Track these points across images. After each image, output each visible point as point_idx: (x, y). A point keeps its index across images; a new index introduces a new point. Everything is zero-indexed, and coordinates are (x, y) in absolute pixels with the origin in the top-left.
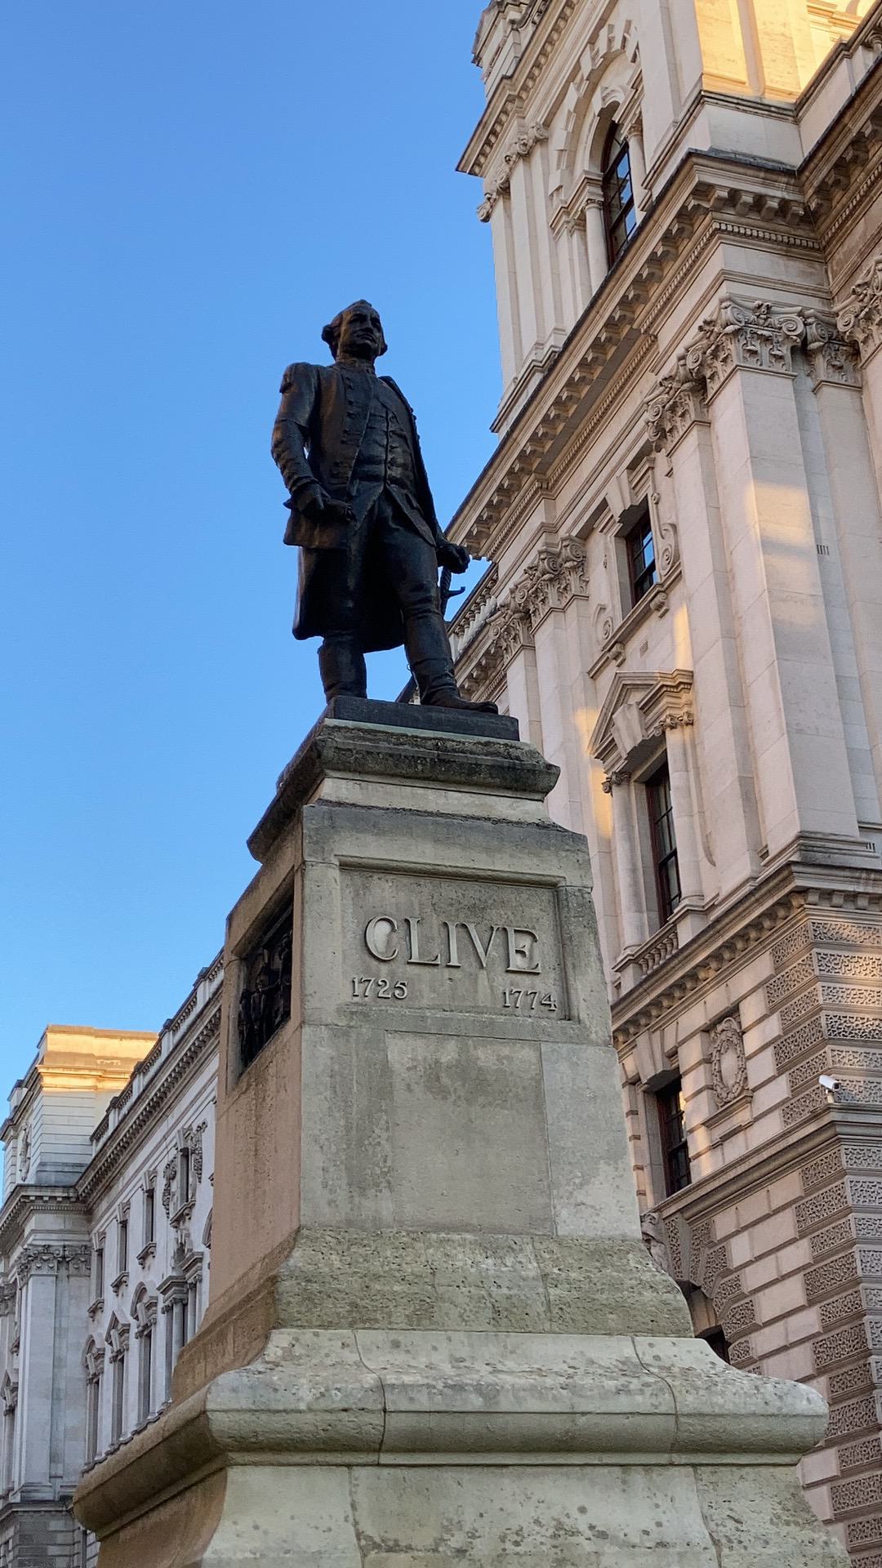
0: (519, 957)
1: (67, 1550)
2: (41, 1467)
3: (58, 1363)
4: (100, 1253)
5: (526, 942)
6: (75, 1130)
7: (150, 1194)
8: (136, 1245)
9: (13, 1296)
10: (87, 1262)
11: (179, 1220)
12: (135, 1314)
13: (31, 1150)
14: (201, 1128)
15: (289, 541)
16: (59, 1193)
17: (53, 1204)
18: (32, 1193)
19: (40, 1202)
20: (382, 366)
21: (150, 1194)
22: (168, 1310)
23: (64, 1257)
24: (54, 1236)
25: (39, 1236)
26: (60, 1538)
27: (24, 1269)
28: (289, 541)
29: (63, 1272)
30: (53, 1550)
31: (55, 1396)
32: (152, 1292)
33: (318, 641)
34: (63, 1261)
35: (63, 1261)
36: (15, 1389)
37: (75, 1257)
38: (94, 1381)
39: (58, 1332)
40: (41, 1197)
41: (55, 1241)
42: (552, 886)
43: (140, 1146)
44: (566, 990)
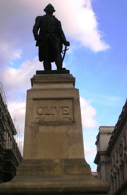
0: (65, 112)
4: (111, 161)
5: (66, 109)
7: (117, 152)
8: (116, 160)
11: (121, 156)
12: (117, 171)
14: (122, 141)
15: (36, 46)
16: (104, 153)
20: (54, 14)
21: (117, 152)
22: (121, 170)
24: (104, 159)
28: (36, 46)
32: (118, 167)
33: (43, 61)
35: (106, 163)
38: (113, 181)
41: (104, 160)
42: (72, 99)
43: (115, 144)
44: (74, 116)
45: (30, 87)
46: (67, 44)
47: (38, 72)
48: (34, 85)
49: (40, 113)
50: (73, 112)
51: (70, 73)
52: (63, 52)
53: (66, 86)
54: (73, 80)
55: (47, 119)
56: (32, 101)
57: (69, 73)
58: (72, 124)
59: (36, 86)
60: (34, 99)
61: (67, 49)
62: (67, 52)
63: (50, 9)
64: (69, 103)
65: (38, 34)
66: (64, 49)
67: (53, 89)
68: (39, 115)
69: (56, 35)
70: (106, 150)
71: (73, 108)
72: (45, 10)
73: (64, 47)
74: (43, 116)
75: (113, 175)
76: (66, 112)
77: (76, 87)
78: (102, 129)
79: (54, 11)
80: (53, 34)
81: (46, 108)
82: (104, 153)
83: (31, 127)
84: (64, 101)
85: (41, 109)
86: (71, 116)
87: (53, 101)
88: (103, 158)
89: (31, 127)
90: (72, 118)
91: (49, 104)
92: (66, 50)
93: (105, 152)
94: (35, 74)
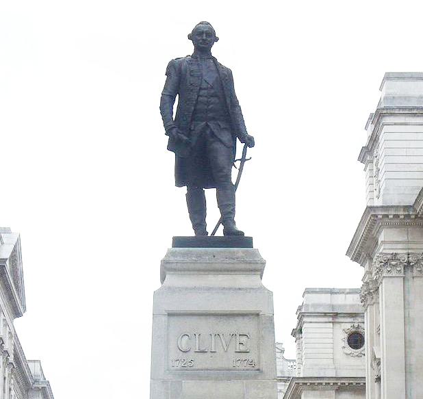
5: (243, 339)
9: (377, 289)
13: (380, 175)
16: (401, 213)
17: (397, 221)
19: (387, 220)
23: (409, 262)
24: (400, 246)
25: (387, 246)
27: (379, 270)
29: (409, 274)
36: (379, 364)
40: (387, 216)
41: (401, 251)
44: (259, 357)
46: (249, 142)
47: (179, 242)
49: (184, 348)
53: (243, 281)
54: (259, 266)
55: (201, 362)
56: (164, 319)
58: (255, 377)
59: (172, 280)
60: (170, 315)
61: (246, 158)
62: (246, 162)
63: (203, 38)
65: (174, 117)
66: (239, 155)
67: (213, 290)
68: (181, 353)
69: (222, 127)
70: (410, 200)
72: (190, 37)
73: (240, 146)
74: (191, 355)
76: (242, 348)
78: (398, 88)
79: (217, 39)
80: (211, 125)
81: (197, 336)
82: (401, 213)
83: (164, 382)
84: (240, 320)
87: (212, 320)
88: (391, 241)
89: (164, 382)
91: (205, 326)
92: (243, 160)
93: (406, 208)
94: (170, 246)
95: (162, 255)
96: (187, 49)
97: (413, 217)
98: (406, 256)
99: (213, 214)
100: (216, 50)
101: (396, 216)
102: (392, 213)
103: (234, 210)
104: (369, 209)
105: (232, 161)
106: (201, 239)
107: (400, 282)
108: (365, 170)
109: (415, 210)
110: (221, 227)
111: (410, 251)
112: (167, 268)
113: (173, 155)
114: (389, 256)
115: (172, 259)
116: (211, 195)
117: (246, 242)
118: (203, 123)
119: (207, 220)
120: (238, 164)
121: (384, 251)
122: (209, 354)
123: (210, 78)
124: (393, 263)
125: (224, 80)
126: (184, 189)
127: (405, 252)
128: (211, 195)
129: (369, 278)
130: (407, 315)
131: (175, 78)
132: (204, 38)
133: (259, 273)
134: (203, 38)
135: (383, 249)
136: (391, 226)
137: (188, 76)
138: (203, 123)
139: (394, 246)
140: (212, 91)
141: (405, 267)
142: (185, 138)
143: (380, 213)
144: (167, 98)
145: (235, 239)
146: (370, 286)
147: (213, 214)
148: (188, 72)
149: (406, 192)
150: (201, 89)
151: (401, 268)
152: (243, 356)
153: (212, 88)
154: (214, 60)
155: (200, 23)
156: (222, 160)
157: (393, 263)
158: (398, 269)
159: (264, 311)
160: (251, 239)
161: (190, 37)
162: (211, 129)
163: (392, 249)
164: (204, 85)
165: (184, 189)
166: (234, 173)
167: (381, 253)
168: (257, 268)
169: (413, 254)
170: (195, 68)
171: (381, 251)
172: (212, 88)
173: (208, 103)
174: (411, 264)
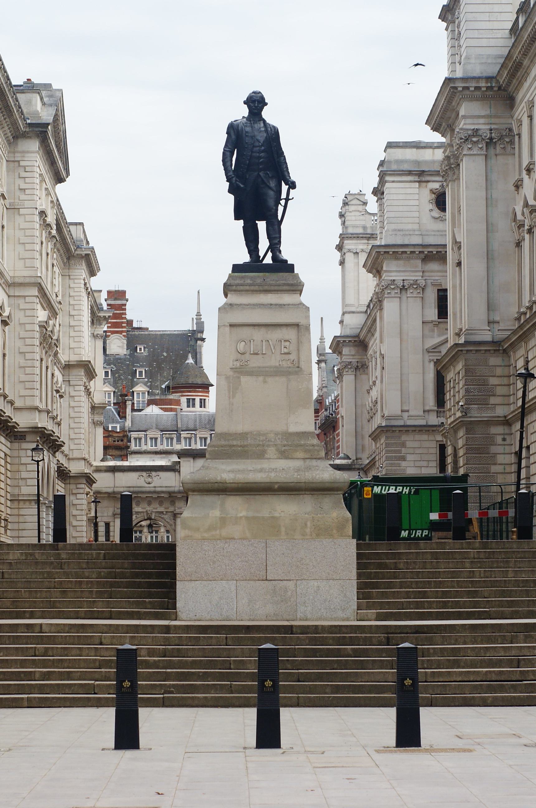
1: (505, 381)
2: (481, 314)
3: (490, 228)
4: (519, 135)
5: (287, 344)
6: (496, 25)
9: (459, 165)
10: (512, 142)
16: (483, 84)
17: (478, 93)
18: (460, 85)
19: (467, 92)
23: (491, 139)
24: (482, 121)
25: (469, 121)
26: (499, 371)
29: (492, 151)
30: (493, 381)
31: (490, 256)
34: (490, 142)
35: (490, 142)
36: (459, 248)
37: (501, 138)
38: (518, 244)
39: (489, 202)
40: (467, 88)
41: (483, 126)
42: (297, 325)
45: (223, 300)
46: (292, 185)
47: (236, 268)
48: (229, 296)
50: (298, 350)
51: (296, 271)
52: (283, 202)
53: (287, 299)
54: (300, 288)
55: (255, 362)
56: (228, 329)
57: (293, 271)
58: (296, 373)
59: (234, 298)
60: (231, 326)
61: (290, 198)
62: (289, 202)
63: (256, 103)
64: (291, 334)
66: (284, 196)
69: (270, 175)
70: (493, 70)
71: (299, 342)
72: (245, 103)
73: (285, 188)
74: (247, 356)
75: (519, 217)
77: (305, 298)
79: (266, 104)
81: (252, 341)
82: (483, 84)
85: (243, 343)
86: (293, 357)
87: (263, 330)
88: (472, 115)
89: (227, 378)
90: (296, 360)
91: (258, 335)
92: (287, 199)
93: (489, 79)
95: (225, 279)
96: (242, 112)
97: (496, 89)
98: (488, 132)
99: (264, 243)
100: (266, 114)
101: (477, 88)
102: (473, 84)
103: (280, 242)
104: (448, 80)
105: (278, 203)
106: (255, 265)
107: (481, 160)
108: (447, 29)
109: (498, 81)
110: (270, 254)
111: (493, 126)
112: (227, 289)
113: (232, 197)
114: (470, 132)
115: (232, 282)
116: (262, 226)
117: (290, 268)
118: (256, 171)
119: (260, 246)
120: (283, 202)
121: (464, 127)
122: (262, 356)
123: (261, 137)
124: (474, 139)
125: (273, 136)
126: (241, 223)
127: (488, 127)
128: (262, 226)
129: (450, 151)
130: (489, 197)
131: (233, 137)
132: (256, 105)
133: (299, 292)
134: (256, 103)
135: (464, 125)
136: (472, 99)
137: (244, 136)
138: (256, 171)
139: (476, 121)
140: (263, 148)
141: (487, 144)
142: (242, 186)
143: (460, 85)
144: (228, 154)
145: (283, 266)
146: (452, 161)
147: (264, 243)
148: (244, 132)
149: (489, 61)
150: (254, 146)
151: (482, 145)
152: (287, 357)
153: (262, 146)
154: (264, 121)
155: (253, 93)
156: (271, 203)
157: (474, 139)
158: (480, 146)
159: (302, 322)
160: (292, 266)
161: (245, 103)
162: (262, 178)
163: (474, 124)
164: (257, 144)
165: (241, 223)
166: (280, 209)
167: (461, 129)
168: (297, 287)
169: (495, 129)
170: (248, 129)
171: (461, 126)
172: (262, 146)
173: (260, 158)
174: (494, 141)
